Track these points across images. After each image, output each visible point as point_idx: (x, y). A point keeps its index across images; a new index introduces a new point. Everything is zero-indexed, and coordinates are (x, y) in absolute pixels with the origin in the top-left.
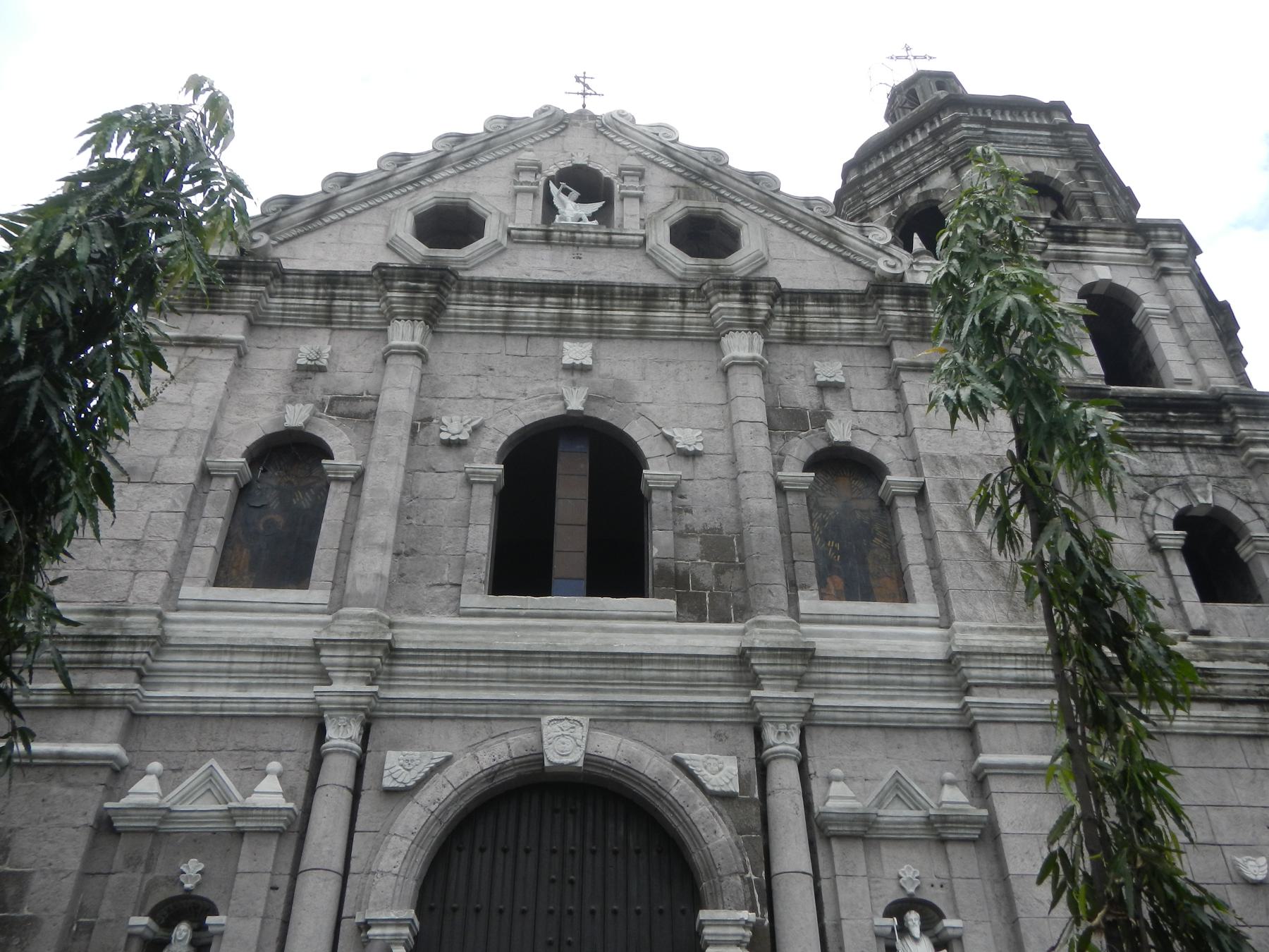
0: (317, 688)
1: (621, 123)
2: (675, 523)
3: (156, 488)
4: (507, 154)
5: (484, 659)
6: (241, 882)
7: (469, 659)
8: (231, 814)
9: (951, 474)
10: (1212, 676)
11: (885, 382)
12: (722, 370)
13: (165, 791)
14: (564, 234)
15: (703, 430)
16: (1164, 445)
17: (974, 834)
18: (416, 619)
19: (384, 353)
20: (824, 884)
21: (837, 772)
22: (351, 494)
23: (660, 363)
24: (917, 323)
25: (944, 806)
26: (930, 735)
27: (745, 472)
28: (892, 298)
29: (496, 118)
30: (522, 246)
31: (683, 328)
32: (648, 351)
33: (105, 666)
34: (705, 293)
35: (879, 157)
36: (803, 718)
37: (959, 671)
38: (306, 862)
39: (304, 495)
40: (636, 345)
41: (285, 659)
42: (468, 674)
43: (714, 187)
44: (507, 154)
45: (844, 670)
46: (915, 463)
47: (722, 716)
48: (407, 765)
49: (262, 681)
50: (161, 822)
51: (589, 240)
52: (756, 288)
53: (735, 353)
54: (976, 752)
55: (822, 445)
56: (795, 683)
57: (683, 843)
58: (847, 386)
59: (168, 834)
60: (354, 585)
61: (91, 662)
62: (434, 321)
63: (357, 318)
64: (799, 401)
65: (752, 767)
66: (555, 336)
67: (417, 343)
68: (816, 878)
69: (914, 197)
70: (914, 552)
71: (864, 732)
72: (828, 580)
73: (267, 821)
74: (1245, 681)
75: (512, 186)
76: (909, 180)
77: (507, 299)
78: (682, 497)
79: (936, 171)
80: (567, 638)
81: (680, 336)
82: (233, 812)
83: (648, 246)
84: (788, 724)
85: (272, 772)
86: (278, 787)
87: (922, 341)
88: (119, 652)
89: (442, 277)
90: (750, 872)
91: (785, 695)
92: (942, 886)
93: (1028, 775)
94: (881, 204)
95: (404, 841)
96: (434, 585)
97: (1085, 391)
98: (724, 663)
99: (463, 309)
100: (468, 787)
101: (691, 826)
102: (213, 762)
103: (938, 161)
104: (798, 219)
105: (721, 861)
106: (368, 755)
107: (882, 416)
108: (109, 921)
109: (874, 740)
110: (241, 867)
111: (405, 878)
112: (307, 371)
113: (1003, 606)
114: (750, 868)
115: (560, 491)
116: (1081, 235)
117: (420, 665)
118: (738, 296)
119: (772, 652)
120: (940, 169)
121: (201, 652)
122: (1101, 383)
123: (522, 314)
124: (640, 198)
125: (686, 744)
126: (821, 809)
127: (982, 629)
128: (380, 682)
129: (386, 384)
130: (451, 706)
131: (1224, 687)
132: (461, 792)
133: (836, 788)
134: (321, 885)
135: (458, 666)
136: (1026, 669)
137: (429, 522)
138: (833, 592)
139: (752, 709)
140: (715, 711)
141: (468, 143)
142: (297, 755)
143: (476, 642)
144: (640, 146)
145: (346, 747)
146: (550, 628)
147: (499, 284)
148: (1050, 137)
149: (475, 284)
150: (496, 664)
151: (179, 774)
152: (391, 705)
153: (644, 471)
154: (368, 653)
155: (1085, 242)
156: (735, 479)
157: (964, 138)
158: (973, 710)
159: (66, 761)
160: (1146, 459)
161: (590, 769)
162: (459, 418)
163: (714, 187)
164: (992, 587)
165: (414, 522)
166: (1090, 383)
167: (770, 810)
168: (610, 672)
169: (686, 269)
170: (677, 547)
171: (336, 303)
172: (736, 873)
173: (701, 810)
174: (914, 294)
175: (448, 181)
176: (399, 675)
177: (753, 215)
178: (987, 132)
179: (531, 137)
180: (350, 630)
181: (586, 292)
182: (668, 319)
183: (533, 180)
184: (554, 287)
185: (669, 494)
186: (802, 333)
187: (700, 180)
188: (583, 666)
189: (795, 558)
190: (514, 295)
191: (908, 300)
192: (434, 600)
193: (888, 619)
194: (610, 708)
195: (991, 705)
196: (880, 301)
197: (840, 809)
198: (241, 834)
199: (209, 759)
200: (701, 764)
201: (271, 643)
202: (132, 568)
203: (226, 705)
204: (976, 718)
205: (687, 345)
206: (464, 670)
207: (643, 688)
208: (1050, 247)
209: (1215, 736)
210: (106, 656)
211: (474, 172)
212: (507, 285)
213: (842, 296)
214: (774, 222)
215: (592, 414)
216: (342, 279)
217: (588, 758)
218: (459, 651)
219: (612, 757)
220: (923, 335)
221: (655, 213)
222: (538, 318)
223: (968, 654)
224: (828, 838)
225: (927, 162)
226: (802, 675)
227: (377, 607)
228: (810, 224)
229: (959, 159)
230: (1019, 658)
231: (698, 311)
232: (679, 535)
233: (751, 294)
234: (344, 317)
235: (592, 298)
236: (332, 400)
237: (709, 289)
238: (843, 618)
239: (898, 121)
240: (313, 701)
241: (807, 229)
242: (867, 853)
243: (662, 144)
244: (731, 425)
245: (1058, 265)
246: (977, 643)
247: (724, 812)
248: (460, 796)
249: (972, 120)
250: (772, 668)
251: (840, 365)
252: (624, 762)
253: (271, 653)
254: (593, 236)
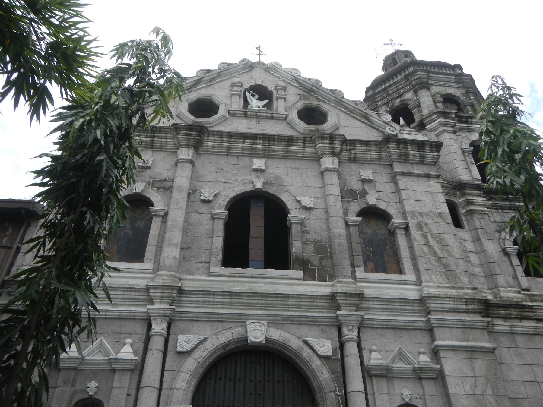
0: (148, 307)
1: (276, 67)
2: (302, 238)
4: (228, 79)
5: (220, 295)
6: (114, 392)
7: (214, 295)
8: (110, 362)
9: (420, 219)
10: (532, 309)
11: (390, 180)
12: (321, 172)
14: (253, 113)
15: (313, 198)
16: (508, 209)
17: (434, 376)
18: (191, 277)
19: (176, 162)
20: (370, 397)
21: (374, 347)
22: (162, 222)
23: (294, 169)
24: (403, 155)
25: (421, 363)
26: (414, 332)
27: (332, 217)
28: (393, 144)
29: (223, 63)
30: (235, 117)
31: (304, 154)
32: (289, 164)
34: (314, 140)
35: (382, 85)
36: (359, 324)
37: (426, 304)
38: (143, 384)
39: (141, 222)
40: (284, 161)
41: (134, 293)
42: (213, 302)
43: (316, 95)
44: (228, 79)
45: (376, 303)
46: (404, 214)
47: (324, 322)
48: (187, 341)
49: (123, 303)
51: (263, 116)
52: (336, 138)
53: (327, 166)
54: (433, 339)
55: (364, 206)
56: (355, 308)
57: (308, 378)
58: (374, 181)
59: (82, 370)
60: (164, 262)
62: (197, 149)
63: (164, 146)
64: (354, 187)
65: (337, 345)
66: (249, 156)
67: (190, 157)
68: (366, 394)
69: (397, 102)
70: (404, 253)
71: (385, 330)
72: (368, 264)
73: (126, 365)
75: (230, 92)
76: (395, 95)
77: (229, 140)
78: (305, 227)
79: (407, 92)
80: (257, 287)
81: (303, 158)
82: (111, 361)
83: (288, 119)
84: (353, 326)
85: (128, 343)
86: (130, 350)
87: (405, 162)
89: (201, 130)
90: (338, 391)
91: (351, 313)
92: (420, 398)
93: (456, 350)
94: (383, 105)
95: (187, 375)
96: (198, 262)
98: (324, 299)
99: (210, 144)
100: (215, 351)
101: (312, 370)
102: (102, 338)
103: (408, 87)
104: (352, 110)
105: (325, 386)
106: (170, 336)
107: (389, 194)
109: (389, 334)
110: (114, 385)
111: (187, 391)
112: (142, 168)
113: (443, 276)
114: (337, 389)
115: (252, 223)
116: (470, 120)
117: (192, 297)
118: (328, 141)
119: (345, 294)
120: (409, 91)
122: (480, 182)
123: (235, 147)
124: (285, 99)
125: (309, 334)
126: (368, 363)
127: (435, 287)
128: (175, 304)
129: (177, 175)
130: (207, 315)
132: (211, 354)
133: (374, 355)
134: (150, 394)
135: (209, 298)
136: (454, 304)
137: (196, 235)
138: (370, 269)
139: (337, 319)
140: (321, 320)
141: (211, 74)
142: (138, 336)
143: (217, 288)
144: (284, 77)
145: (161, 333)
146: (249, 282)
147: (226, 134)
148: (455, 79)
149: (215, 133)
150: (226, 297)
151: (87, 343)
152: (180, 315)
153: (289, 215)
154: (170, 291)
155: (471, 123)
156: (327, 219)
157: (419, 78)
158: (432, 322)
160: (500, 215)
161: (268, 344)
162: (208, 190)
163: (316, 95)
164: (439, 268)
165: (189, 235)
166: (476, 182)
167: (345, 364)
168: (275, 302)
169: (305, 130)
170: (303, 248)
171: (155, 139)
172: (332, 391)
173: (316, 363)
174: (402, 143)
175: (203, 90)
176: (183, 301)
177: (333, 108)
178: (428, 76)
179: (238, 72)
180: (163, 281)
181: (262, 138)
182: (298, 150)
183: (239, 90)
184: (249, 135)
185: (299, 225)
186: (354, 158)
187: (310, 92)
188: (264, 299)
189: (354, 254)
190: (232, 138)
191: (400, 145)
192: (198, 269)
193: (394, 281)
194: (275, 318)
195: (440, 319)
196: (388, 145)
197: (376, 364)
198: (114, 370)
199: (100, 337)
200: (315, 343)
201: (127, 286)
203: (107, 313)
204: (433, 325)
205: (306, 161)
206: (212, 300)
207: (290, 309)
208: (457, 124)
209: (534, 335)
211: (213, 86)
212: (229, 134)
213: (372, 143)
214: (341, 111)
215: (266, 190)
216: (158, 129)
217: (267, 339)
218: (210, 291)
219: (277, 339)
220: (406, 160)
221: (291, 105)
222: (242, 149)
223: (429, 297)
224: (371, 377)
225: (403, 88)
226: (358, 305)
227: (174, 271)
228: (357, 112)
229: (417, 87)
230: (451, 299)
231: (310, 147)
232: (304, 243)
233: (333, 141)
234: (158, 146)
235: (265, 141)
236: (153, 181)
237: (315, 138)
238: (375, 280)
239: (388, 71)
240: (146, 312)
241: (356, 114)
242: (388, 384)
243: (294, 76)
244: (325, 196)
245: (461, 132)
246: (433, 293)
247: (326, 364)
248: (211, 355)
249: (422, 71)
250: (345, 302)
251: (371, 172)
252: (282, 342)
253: (127, 291)
254: (265, 114)
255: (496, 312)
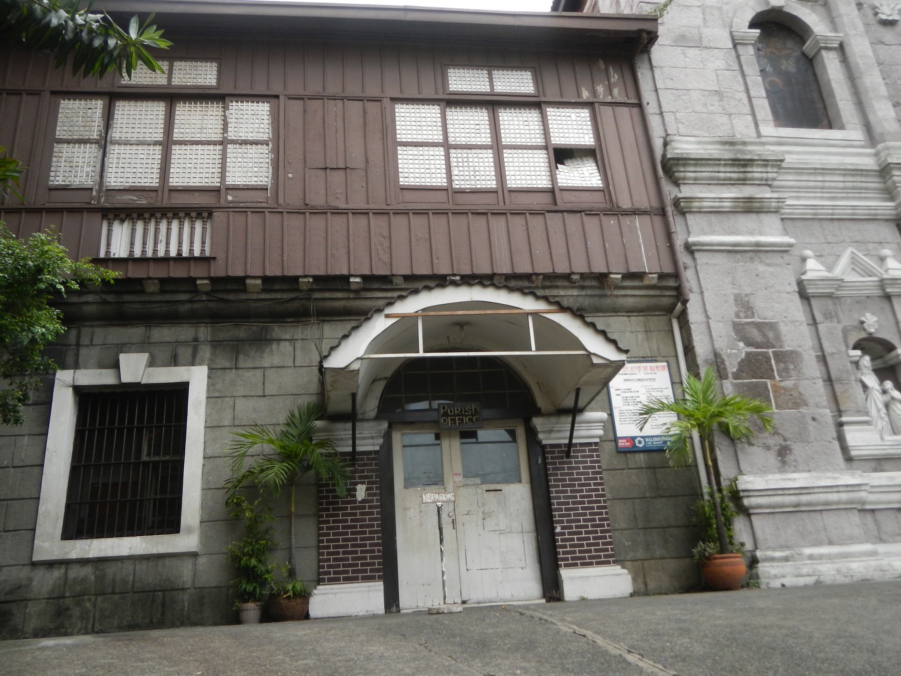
3: (706, 51)
13: (830, 269)
33: (748, 182)
41: (859, 179)
49: (845, 195)
50: (837, 290)
59: (837, 298)
61: (739, 179)
88: (757, 172)
102: (850, 249)
108: (833, 353)
121: (802, 174)
159: (760, 248)
201: (850, 167)
202: (725, 112)
210: (750, 175)
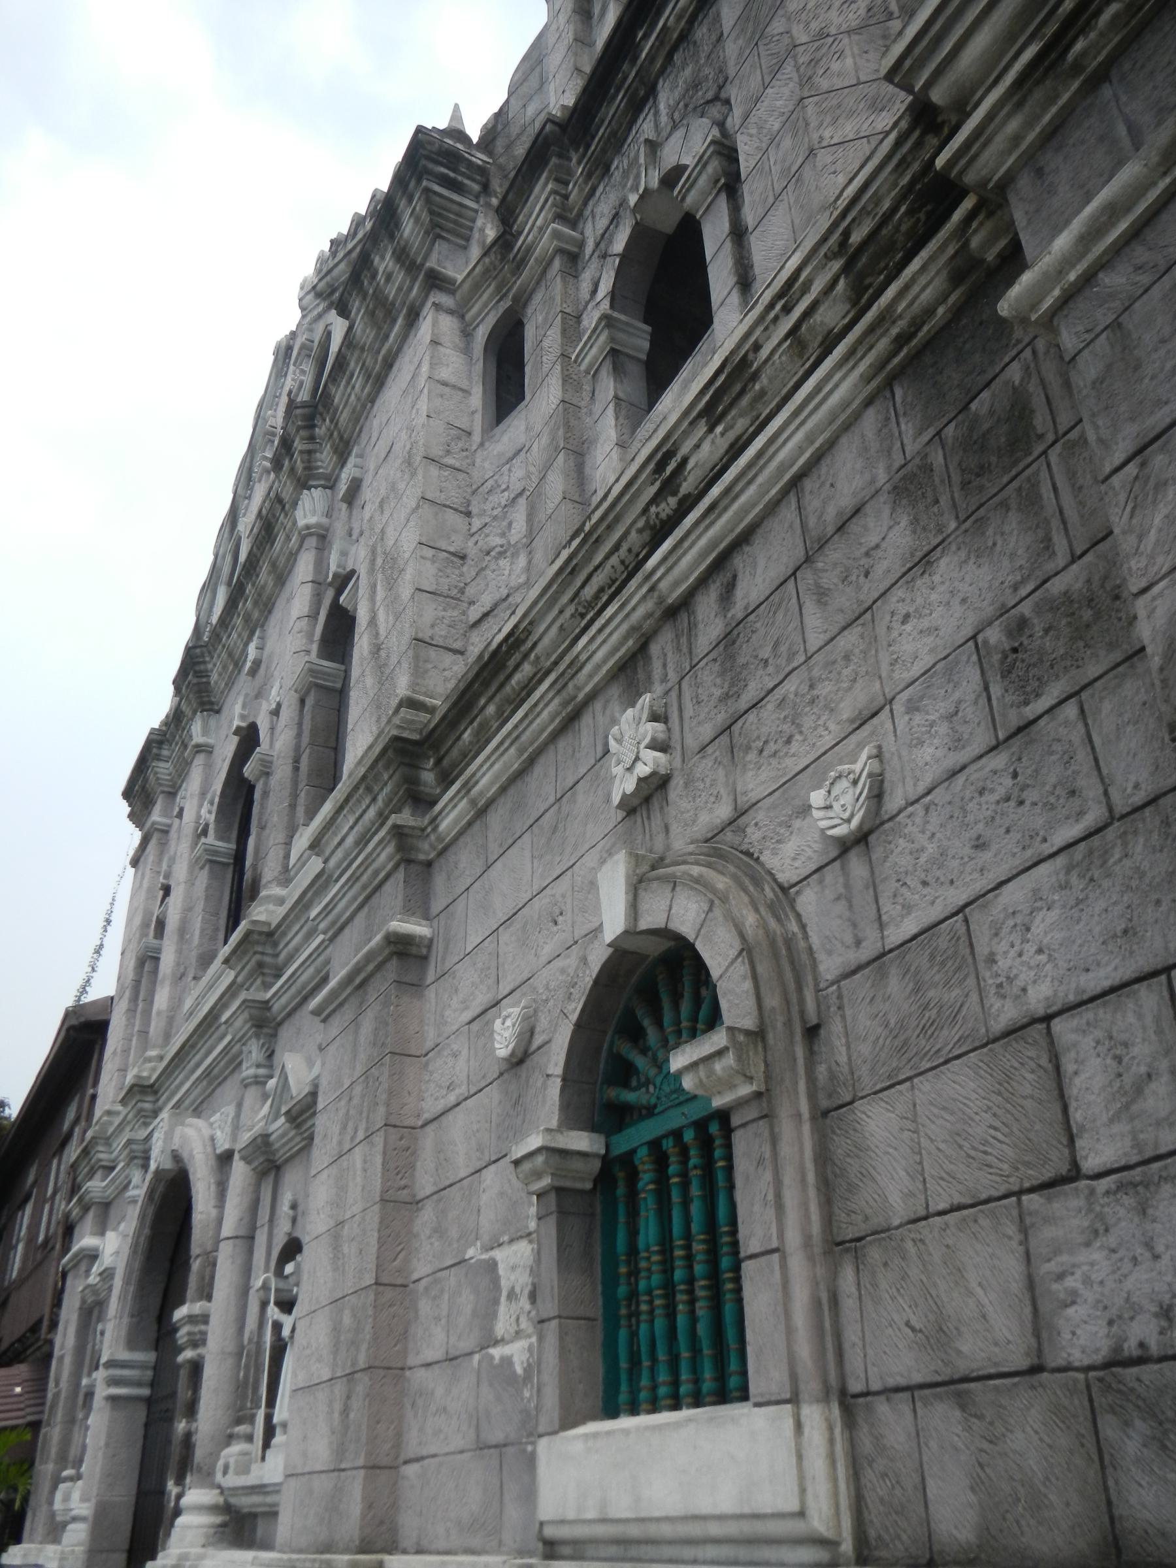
10: (519, 643)
24: (375, 308)
36: (253, 1026)
74: (555, 611)
97: (524, 168)
131: (539, 649)
209: (531, 761)
230: (345, 812)
255: (455, 752)
